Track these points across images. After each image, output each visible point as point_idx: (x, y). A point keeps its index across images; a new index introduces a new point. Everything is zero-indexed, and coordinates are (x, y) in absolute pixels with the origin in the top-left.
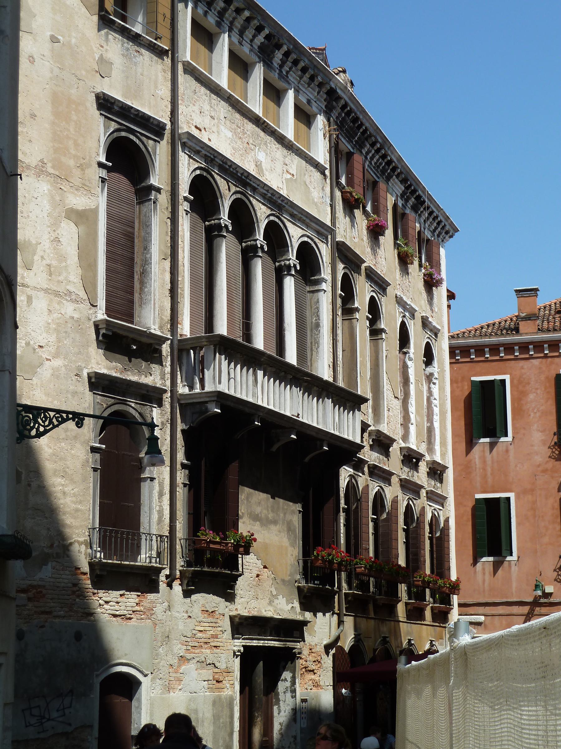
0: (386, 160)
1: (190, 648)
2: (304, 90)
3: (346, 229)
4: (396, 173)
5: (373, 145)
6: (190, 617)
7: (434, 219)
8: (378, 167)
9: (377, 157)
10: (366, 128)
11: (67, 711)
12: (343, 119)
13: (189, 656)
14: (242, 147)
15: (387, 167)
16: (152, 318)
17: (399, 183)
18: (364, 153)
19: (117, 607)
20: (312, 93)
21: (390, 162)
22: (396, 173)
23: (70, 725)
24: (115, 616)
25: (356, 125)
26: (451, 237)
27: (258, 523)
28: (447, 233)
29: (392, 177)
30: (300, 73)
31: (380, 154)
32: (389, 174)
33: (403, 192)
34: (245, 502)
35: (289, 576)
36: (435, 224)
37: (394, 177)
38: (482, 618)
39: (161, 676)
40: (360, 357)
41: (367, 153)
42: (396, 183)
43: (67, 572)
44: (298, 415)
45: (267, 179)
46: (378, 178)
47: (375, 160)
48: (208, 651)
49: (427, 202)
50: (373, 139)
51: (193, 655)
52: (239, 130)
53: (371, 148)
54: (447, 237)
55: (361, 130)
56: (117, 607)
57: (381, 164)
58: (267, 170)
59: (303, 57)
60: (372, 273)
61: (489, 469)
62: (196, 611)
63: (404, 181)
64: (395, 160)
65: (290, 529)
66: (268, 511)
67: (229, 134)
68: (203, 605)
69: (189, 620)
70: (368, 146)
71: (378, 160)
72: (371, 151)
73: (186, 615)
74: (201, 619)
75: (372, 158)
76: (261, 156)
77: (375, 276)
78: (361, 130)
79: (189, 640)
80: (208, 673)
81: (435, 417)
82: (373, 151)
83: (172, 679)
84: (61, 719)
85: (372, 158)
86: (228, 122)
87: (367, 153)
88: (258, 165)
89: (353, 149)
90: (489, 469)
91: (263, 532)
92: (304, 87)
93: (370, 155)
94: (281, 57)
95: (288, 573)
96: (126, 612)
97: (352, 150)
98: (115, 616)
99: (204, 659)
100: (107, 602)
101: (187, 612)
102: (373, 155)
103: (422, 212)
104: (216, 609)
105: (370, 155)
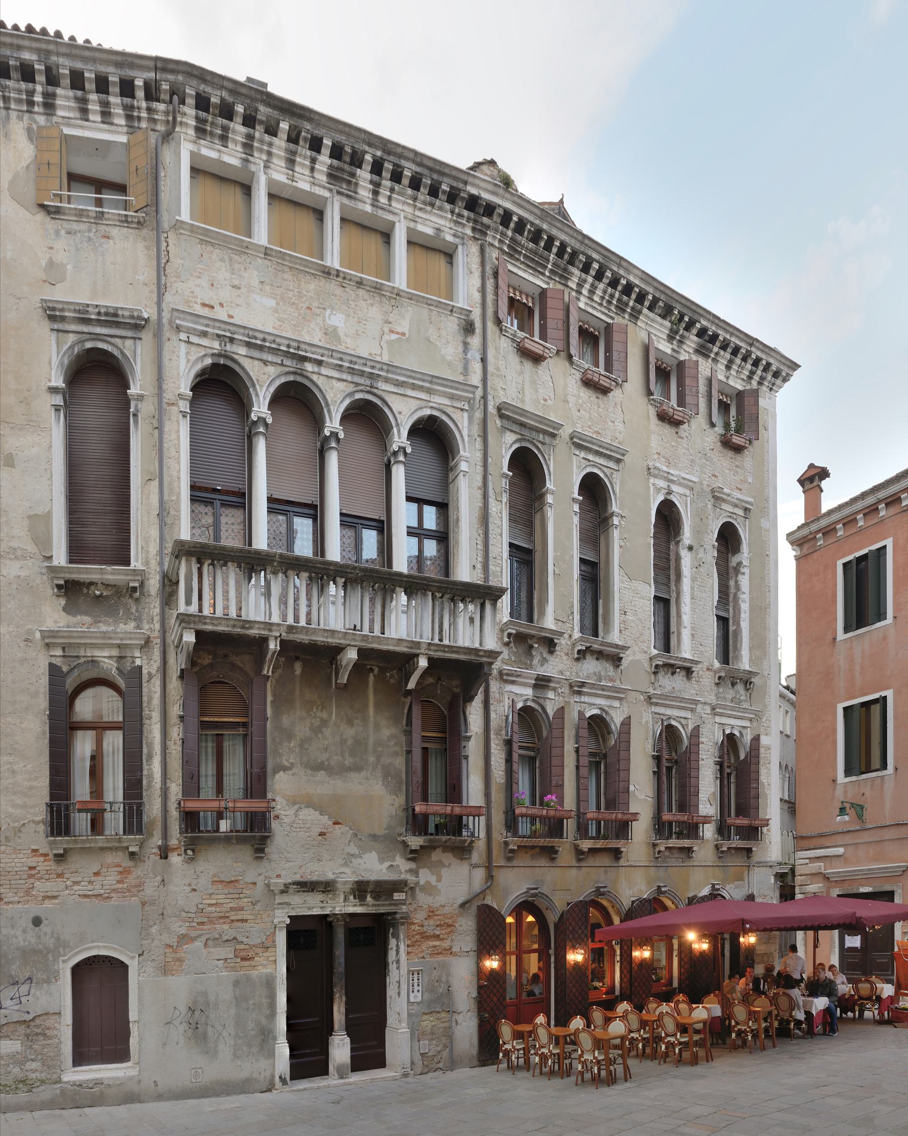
0: (620, 288)
1: (195, 924)
2: (424, 216)
3: (523, 389)
4: (647, 303)
5: (586, 269)
6: (194, 890)
7: (745, 359)
8: (609, 302)
9: (601, 286)
10: (572, 248)
11: (23, 1000)
12: (512, 239)
13: (193, 934)
14: (296, 315)
15: (625, 298)
16: (686, 650)
17: (659, 319)
18: (574, 286)
19: (90, 887)
20: (442, 217)
21: (628, 289)
22: (647, 303)
23: (28, 1013)
24: (86, 896)
25: (542, 244)
26: (785, 380)
27: (322, 772)
28: (776, 375)
29: (640, 312)
30: (410, 191)
31: (606, 281)
32: (633, 308)
33: (671, 330)
34: (297, 750)
35: (386, 829)
36: (749, 366)
37: (645, 311)
38: (841, 851)
39: (153, 957)
40: (555, 550)
41: (580, 286)
42: (653, 320)
43: (21, 856)
44: (355, 626)
45: (347, 348)
46: (613, 318)
47: (599, 292)
48: (226, 927)
49: (722, 335)
50: (582, 258)
51: (198, 932)
52: (291, 294)
53: (584, 275)
54: (778, 382)
55: (555, 250)
56: (90, 887)
57: (612, 296)
58: (346, 335)
59: (404, 163)
60: (584, 440)
61: (858, 668)
62: (204, 882)
63: (667, 312)
64: (637, 282)
65: (387, 773)
66: (343, 756)
67: (272, 303)
68: (214, 876)
69: (195, 893)
70: (576, 272)
71: (605, 292)
72: (585, 281)
73: (188, 889)
74: (211, 891)
75: (592, 292)
76: (337, 320)
77: (593, 444)
78: (555, 250)
79: (193, 915)
80: (227, 952)
81: (742, 615)
82: (590, 279)
83: (168, 960)
84: (16, 1008)
85: (592, 292)
86: (268, 288)
87: (580, 286)
88: (331, 332)
89: (548, 284)
90: (858, 668)
91: (332, 782)
92: (426, 212)
93: (587, 286)
94: (368, 176)
95: (385, 826)
96: (102, 891)
97: (545, 286)
98: (86, 896)
99: (217, 936)
100: (75, 883)
101: (190, 885)
102: (592, 285)
103: (717, 354)
104: (241, 878)
105: (587, 286)
